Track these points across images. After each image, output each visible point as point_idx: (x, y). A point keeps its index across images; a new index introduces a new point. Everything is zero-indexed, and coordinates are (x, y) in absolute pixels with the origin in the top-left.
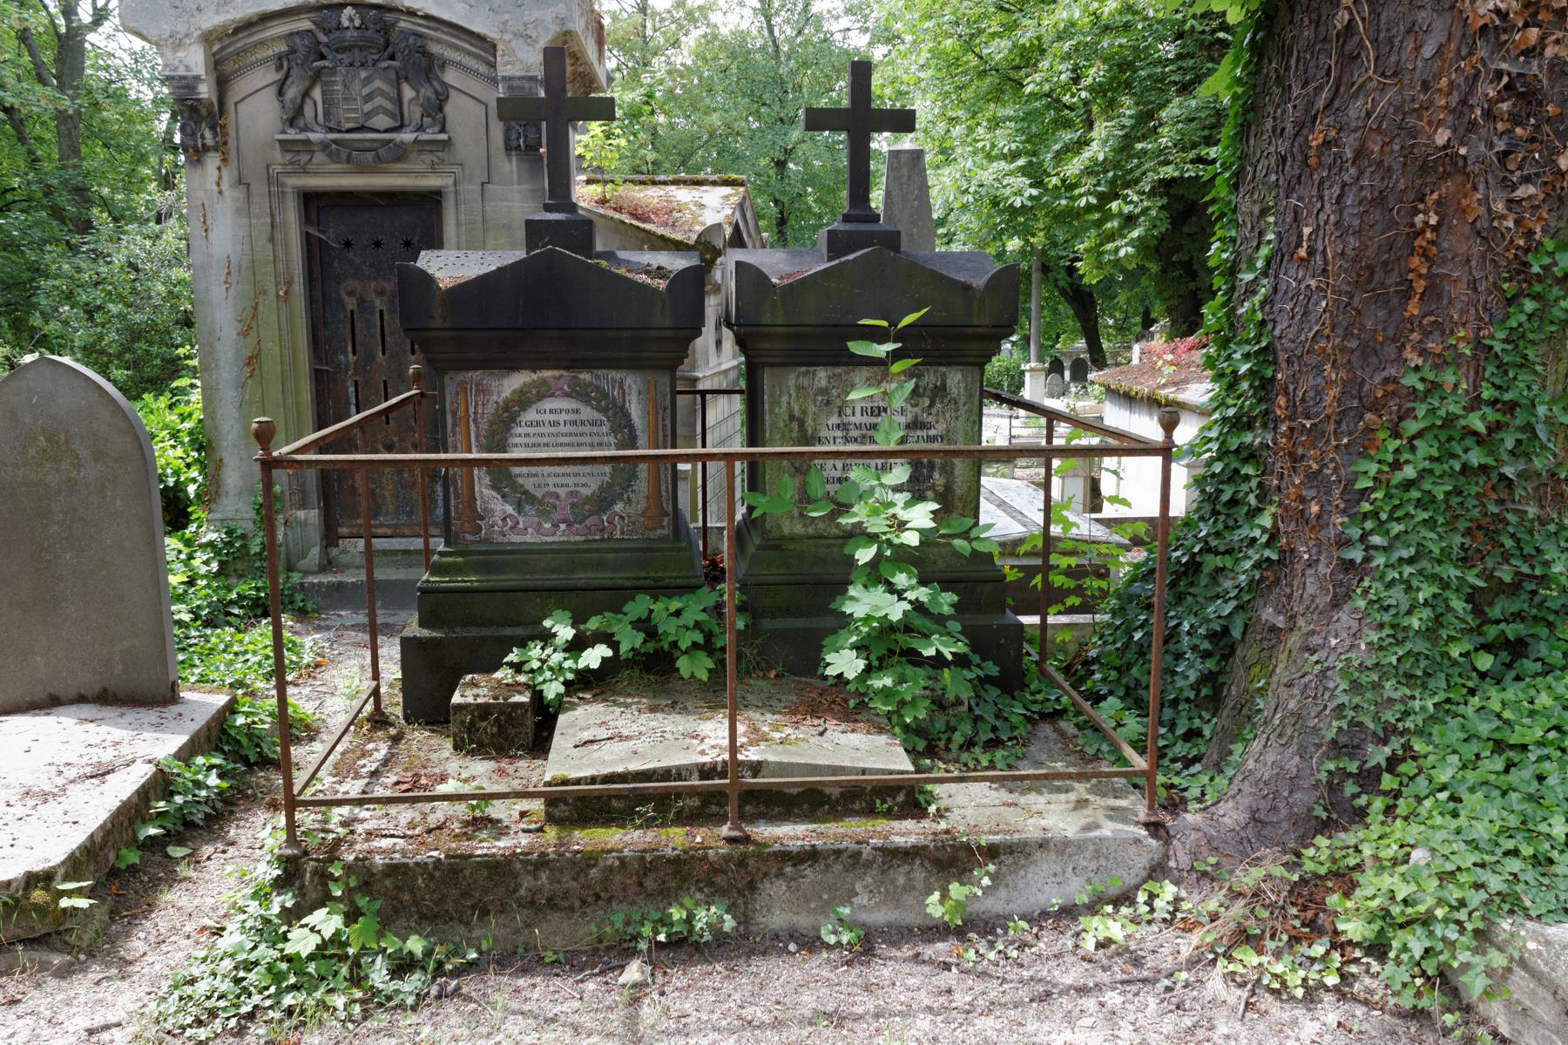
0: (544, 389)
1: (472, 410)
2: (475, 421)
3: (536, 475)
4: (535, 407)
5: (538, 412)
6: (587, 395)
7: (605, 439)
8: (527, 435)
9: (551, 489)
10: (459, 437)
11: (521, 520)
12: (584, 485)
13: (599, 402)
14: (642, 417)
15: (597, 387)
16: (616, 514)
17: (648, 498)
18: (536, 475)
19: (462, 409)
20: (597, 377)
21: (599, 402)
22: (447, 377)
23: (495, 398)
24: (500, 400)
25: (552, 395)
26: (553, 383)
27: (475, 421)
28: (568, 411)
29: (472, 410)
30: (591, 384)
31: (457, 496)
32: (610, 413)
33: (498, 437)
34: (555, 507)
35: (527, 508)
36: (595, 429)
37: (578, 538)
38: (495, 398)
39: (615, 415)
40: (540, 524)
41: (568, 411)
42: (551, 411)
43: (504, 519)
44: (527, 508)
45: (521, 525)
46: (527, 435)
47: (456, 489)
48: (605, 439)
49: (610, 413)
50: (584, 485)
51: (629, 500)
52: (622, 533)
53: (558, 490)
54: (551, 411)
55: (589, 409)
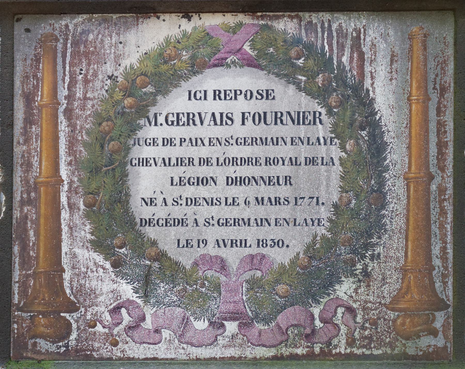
0: (204, 51)
1: (63, 92)
2: (69, 113)
3: (181, 222)
4: (185, 86)
5: (192, 96)
6: (289, 62)
7: (322, 151)
8: (168, 142)
9: (211, 250)
10: (35, 144)
11: (149, 311)
12: (277, 243)
13: (312, 77)
14: (392, 107)
15: (310, 47)
16: (339, 303)
17: (404, 271)
18: (181, 222)
19: (46, 88)
20: (310, 26)
21: (312, 77)
22: (19, 29)
23: (109, 68)
24: (119, 73)
25: (221, 63)
26: (223, 39)
27: (69, 113)
28: (249, 95)
29: (63, 92)
30: (297, 41)
31: (24, 264)
32: (333, 100)
33: (113, 145)
34: (217, 287)
35: (162, 288)
36: (302, 131)
37: (261, 352)
38: (109, 68)
39: (341, 104)
40: (185, 322)
41: (249, 95)
42: (217, 95)
43: (116, 310)
44: (162, 288)
45: (148, 324)
46: (168, 142)
47: (24, 248)
48: (322, 151)
49: (333, 100)
50: (277, 243)
51: (366, 274)
52: (351, 342)
53: (223, 252)
54: (217, 95)
55: (292, 89)
